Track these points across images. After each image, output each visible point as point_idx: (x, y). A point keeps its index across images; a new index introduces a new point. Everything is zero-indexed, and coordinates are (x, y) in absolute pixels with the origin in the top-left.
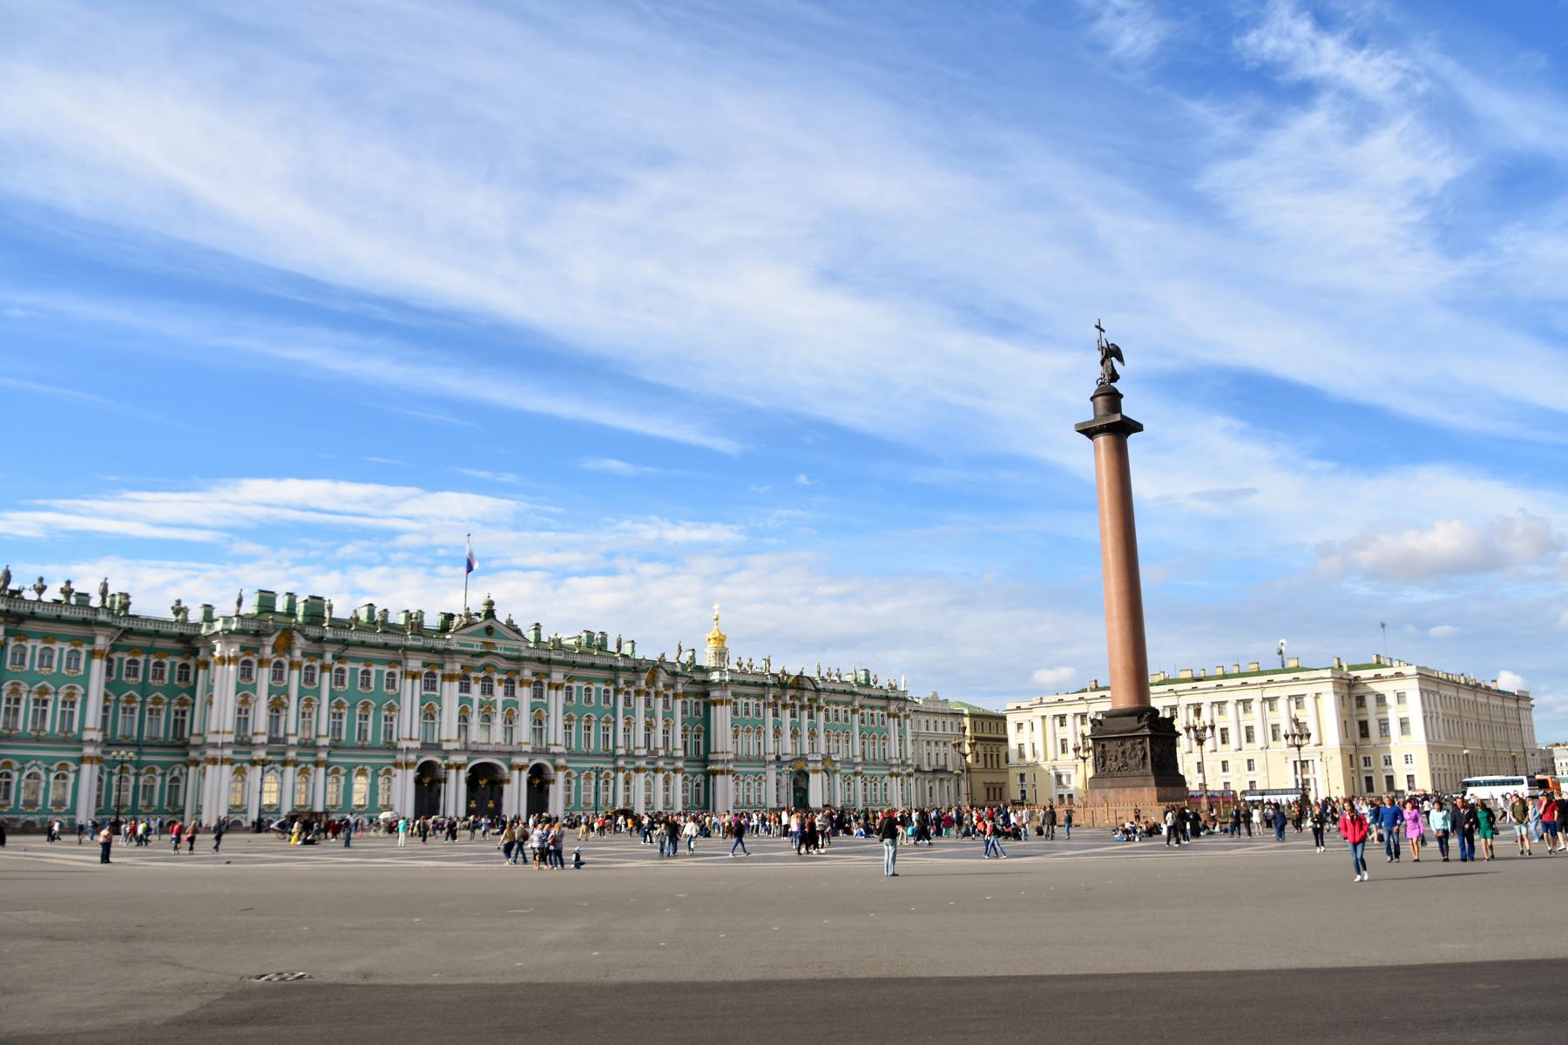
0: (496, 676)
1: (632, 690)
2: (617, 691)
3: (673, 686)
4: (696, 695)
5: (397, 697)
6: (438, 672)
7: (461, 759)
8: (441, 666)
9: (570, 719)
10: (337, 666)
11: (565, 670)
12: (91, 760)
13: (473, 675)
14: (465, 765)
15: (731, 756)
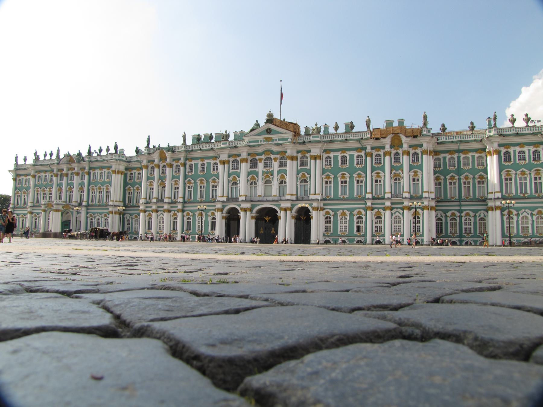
0: (272, 156)
1: (381, 153)
2: (366, 155)
3: (421, 146)
4: (476, 151)
5: (217, 176)
6: (238, 159)
7: (248, 205)
8: (239, 155)
9: (328, 177)
10: (188, 163)
11: (320, 145)
12: (112, 213)
13: (257, 157)
14: (251, 210)
15: (499, 195)
